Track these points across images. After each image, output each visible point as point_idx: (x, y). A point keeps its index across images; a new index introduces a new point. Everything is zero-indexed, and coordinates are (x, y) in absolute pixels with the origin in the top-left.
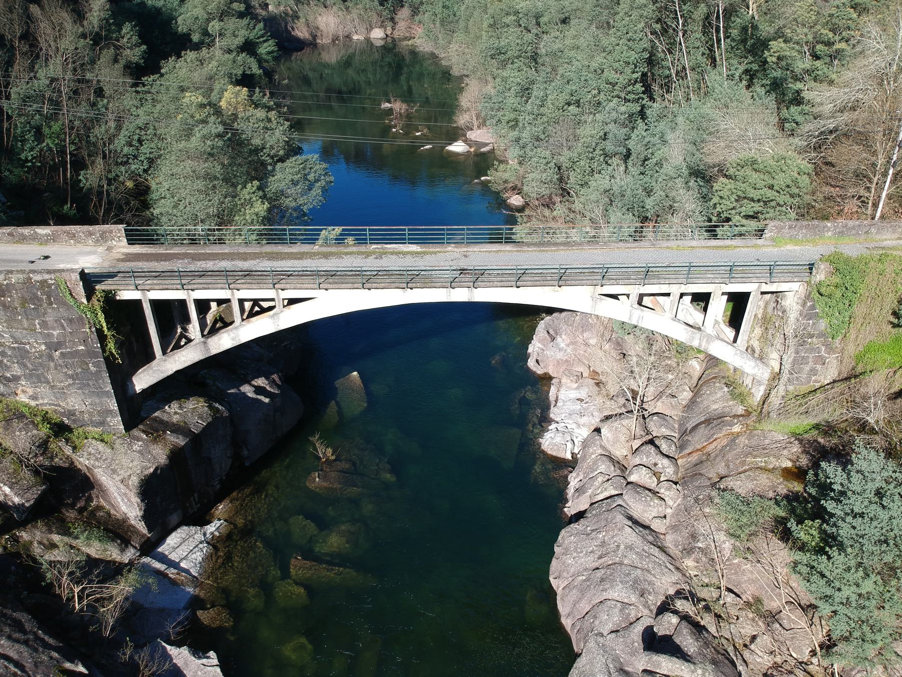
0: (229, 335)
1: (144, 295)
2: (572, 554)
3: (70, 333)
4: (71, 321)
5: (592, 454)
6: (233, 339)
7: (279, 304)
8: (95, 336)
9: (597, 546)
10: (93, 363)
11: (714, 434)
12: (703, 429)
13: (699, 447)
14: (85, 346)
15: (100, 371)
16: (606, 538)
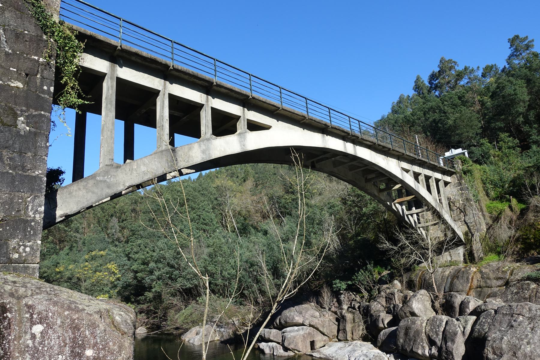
0: (200, 146)
1: (113, 70)
2: (523, 344)
3: (7, 54)
4: (18, 36)
5: (422, 323)
6: (204, 152)
7: (241, 126)
8: (51, 74)
9: (530, 324)
10: (27, 117)
11: (468, 278)
12: (458, 282)
13: (468, 289)
14: (25, 83)
15: (35, 134)
16: (527, 315)
